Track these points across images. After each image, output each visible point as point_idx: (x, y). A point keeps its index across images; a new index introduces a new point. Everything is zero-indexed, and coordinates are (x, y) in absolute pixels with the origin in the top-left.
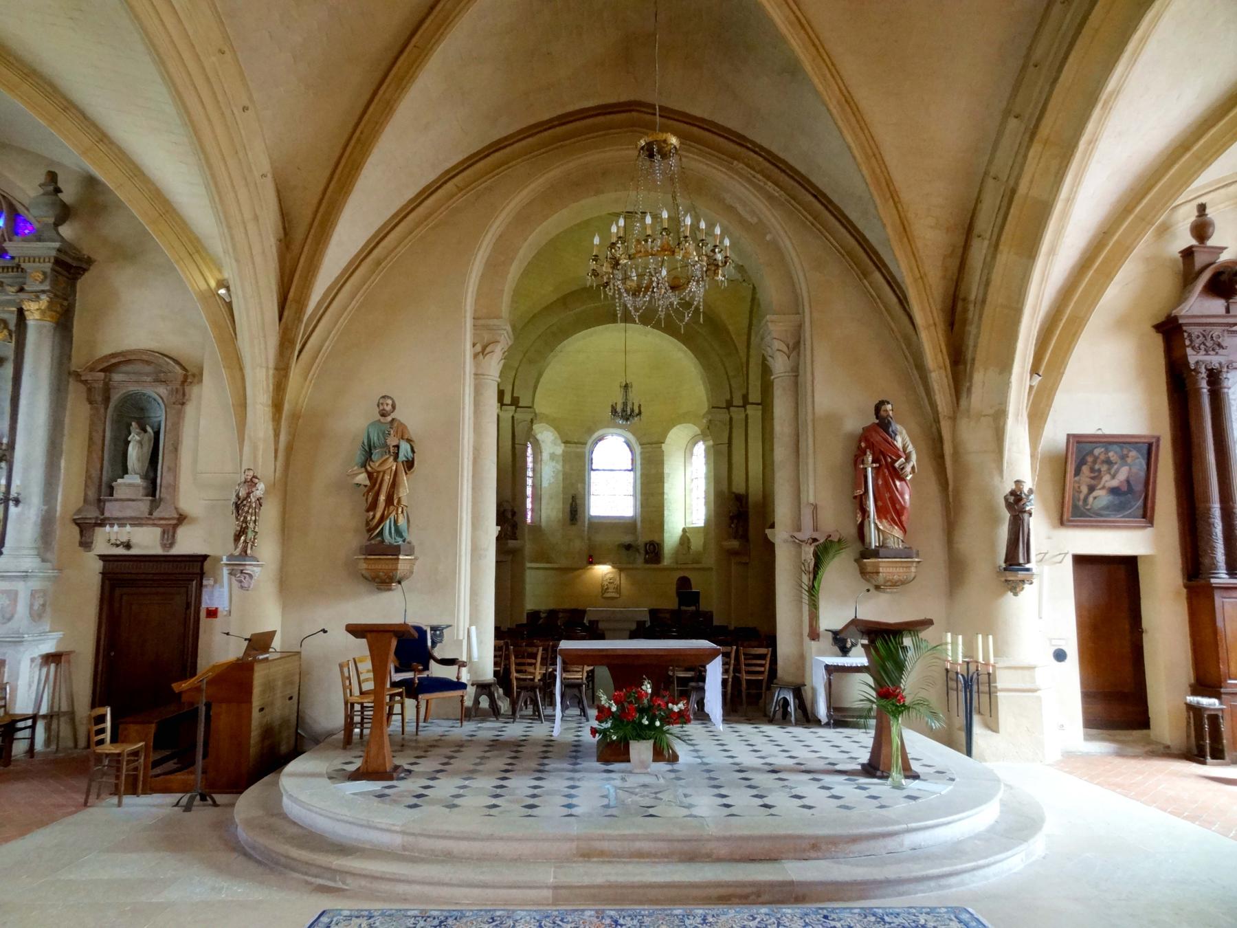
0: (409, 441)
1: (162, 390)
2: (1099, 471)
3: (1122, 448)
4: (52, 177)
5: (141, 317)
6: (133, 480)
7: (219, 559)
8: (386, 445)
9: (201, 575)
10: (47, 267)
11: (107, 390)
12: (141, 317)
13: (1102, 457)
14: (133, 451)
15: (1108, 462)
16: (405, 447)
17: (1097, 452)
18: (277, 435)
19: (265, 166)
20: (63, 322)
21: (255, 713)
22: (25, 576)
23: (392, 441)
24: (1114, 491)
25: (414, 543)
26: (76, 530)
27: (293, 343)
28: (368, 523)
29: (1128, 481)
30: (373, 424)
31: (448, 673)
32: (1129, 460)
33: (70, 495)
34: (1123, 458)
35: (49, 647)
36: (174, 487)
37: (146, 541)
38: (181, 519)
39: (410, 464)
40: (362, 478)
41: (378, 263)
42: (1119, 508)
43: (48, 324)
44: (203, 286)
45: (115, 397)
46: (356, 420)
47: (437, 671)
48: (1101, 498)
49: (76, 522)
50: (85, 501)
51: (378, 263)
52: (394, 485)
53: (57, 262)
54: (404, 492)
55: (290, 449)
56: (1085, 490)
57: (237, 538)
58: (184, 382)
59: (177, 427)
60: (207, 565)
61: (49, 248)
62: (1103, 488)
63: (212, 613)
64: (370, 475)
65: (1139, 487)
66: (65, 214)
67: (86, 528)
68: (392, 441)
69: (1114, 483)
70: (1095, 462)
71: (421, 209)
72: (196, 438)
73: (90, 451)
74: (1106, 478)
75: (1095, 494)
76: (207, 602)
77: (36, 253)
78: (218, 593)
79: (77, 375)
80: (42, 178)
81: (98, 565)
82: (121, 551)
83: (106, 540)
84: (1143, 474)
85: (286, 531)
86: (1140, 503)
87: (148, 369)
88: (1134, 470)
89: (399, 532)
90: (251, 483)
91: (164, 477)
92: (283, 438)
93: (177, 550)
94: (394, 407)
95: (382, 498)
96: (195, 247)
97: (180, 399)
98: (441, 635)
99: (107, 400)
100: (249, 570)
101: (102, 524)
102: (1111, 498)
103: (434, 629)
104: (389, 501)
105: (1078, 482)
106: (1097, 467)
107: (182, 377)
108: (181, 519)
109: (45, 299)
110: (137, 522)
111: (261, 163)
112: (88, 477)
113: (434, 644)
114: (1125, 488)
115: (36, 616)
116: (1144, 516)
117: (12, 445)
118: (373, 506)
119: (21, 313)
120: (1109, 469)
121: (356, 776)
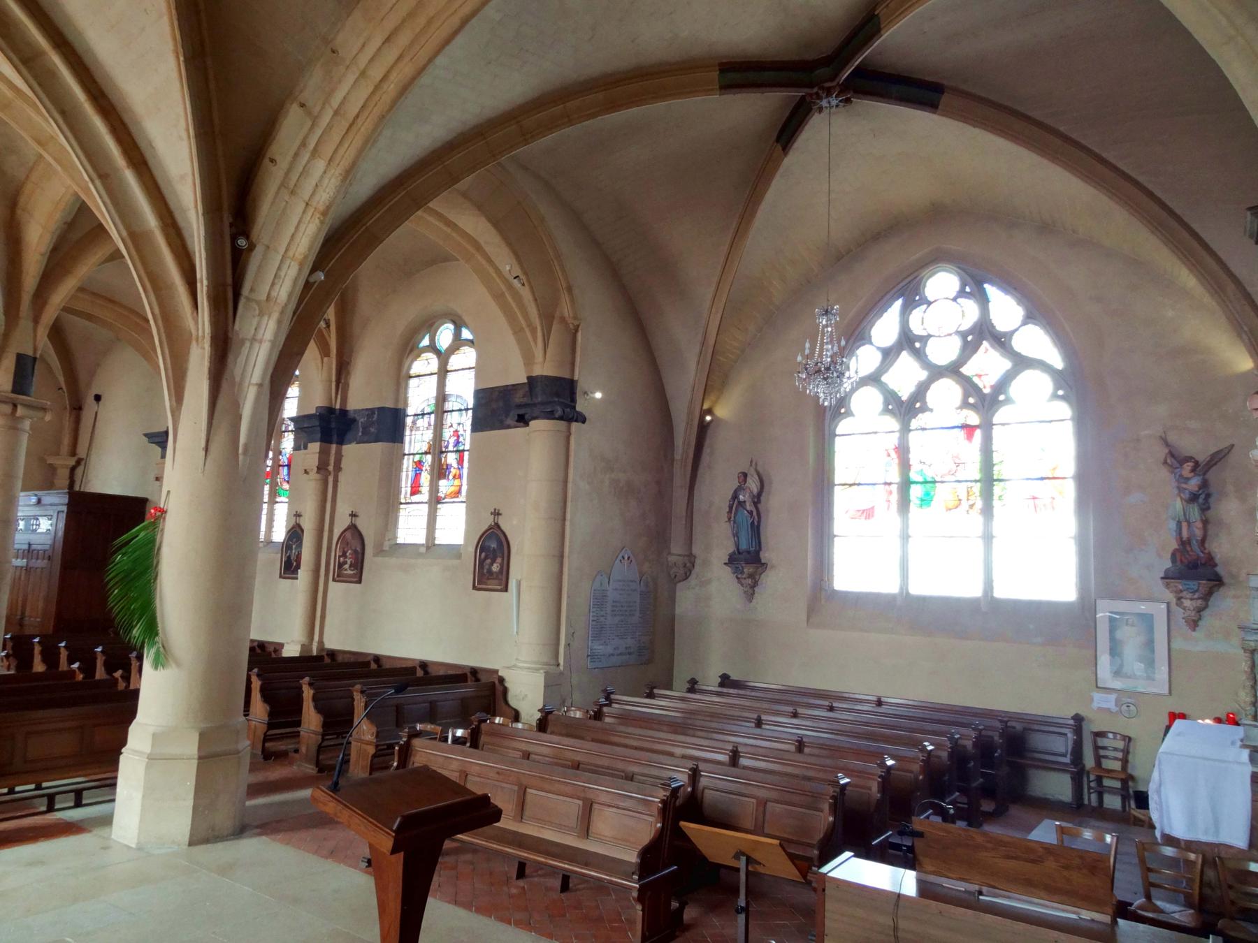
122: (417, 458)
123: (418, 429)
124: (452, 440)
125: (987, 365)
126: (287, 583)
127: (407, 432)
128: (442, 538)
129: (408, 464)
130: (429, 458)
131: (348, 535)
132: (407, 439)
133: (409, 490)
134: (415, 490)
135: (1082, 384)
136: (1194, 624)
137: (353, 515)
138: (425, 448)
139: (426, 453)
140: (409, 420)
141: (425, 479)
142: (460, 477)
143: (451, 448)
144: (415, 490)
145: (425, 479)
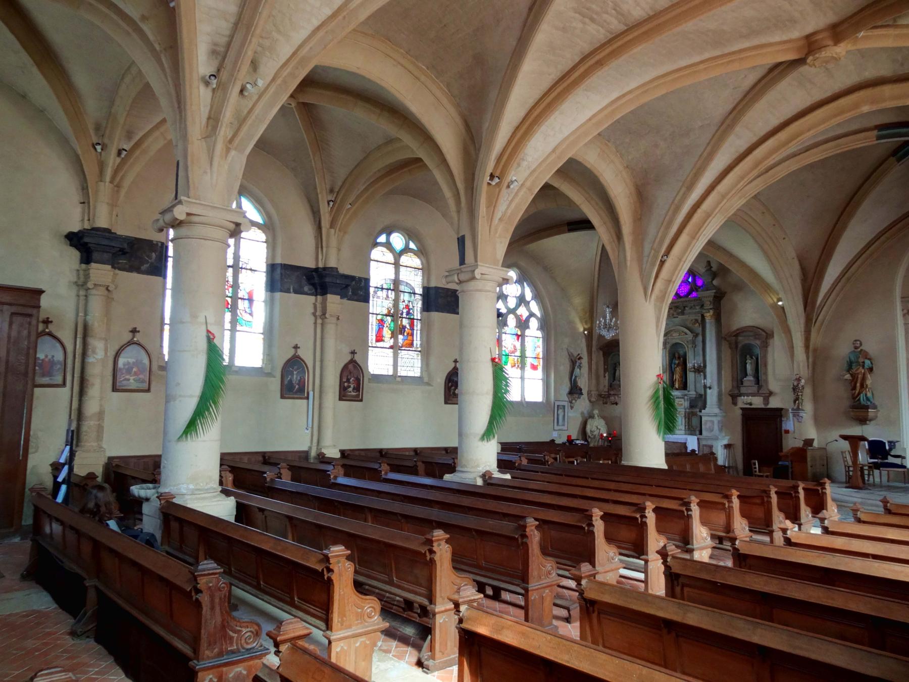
0: (870, 359)
1: (758, 342)
4: (709, 263)
5: (748, 313)
6: (750, 378)
7: (787, 410)
8: (858, 362)
9: (781, 416)
10: (711, 299)
11: (736, 343)
12: (748, 313)
14: (749, 367)
16: (867, 362)
18: (808, 358)
19: (794, 254)
20: (718, 318)
21: (809, 468)
22: (716, 415)
23: (861, 360)
25: (877, 403)
26: (730, 398)
27: (811, 320)
28: (853, 395)
30: (851, 352)
31: (898, 461)
33: (727, 385)
35: (725, 442)
36: (766, 381)
37: (757, 402)
38: (771, 393)
39: (871, 370)
40: (848, 376)
41: (849, 279)
43: (713, 320)
44: (771, 301)
45: (740, 346)
46: (843, 350)
47: (891, 460)
49: (731, 395)
50: (733, 387)
51: (849, 279)
52: (864, 379)
53: (715, 297)
54: (869, 382)
55: (814, 363)
57: (795, 402)
58: (767, 338)
59: (765, 357)
60: (783, 412)
61: (712, 293)
63: (787, 432)
64: (851, 375)
66: (714, 275)
67: (734, 397)
68: (861, 360)
71: (868, 252)
72: (774, 360)
73: (732, 366)
76: (784, 427)
77: (707, 295)
78: (789, 424)
79: (725, 339)
80: (705, 264)
81: (740, 412)
82: (748, 406)
83: (743, 401)
85: (816, 398)
87: (751, 334)
89: (868, 399)
90: (799, 380)
91: (762, 377)
92: (810, 360)
93: (769, 406)
94: (861, 344)
95: (858, 385)
96: (766, 287)
97: (765, 346)
98: (895, 445)
99: (737, 347)
100: (801, 415)
101: (740, 395)
103: (890, 442)
104: (862, 386)
107: (765, 336)
108: (771, 393)
109: (711, 312)
110: (753, 395)
111: (791, 254)
112: (733, 378)
113: (891, 449)
115: (721, 430)
117: (705, 366)
118: (854, 388)
119: (703, 317)
121: (846, 487)
122: (379, 317)
123: (378, 297)
124: (405, 311)
125: (523, 312)
126: (288, 402)
127: (371, 298)
128: (402, 372)
129: (373, 321)
130: (389, 319)
131: (351, 366)
132: (371, 302)
133: (374, 338)
134: (379, 338)
135: (544, 326)
136: (572, 408)
137: (353, 353)
138: (385, 312)
139: (386, 315)
140: (372, 290)
141: (387, 333)
142: (412, 335)
143: (404, 315)
144: (379, 338)
145: (387, 333)
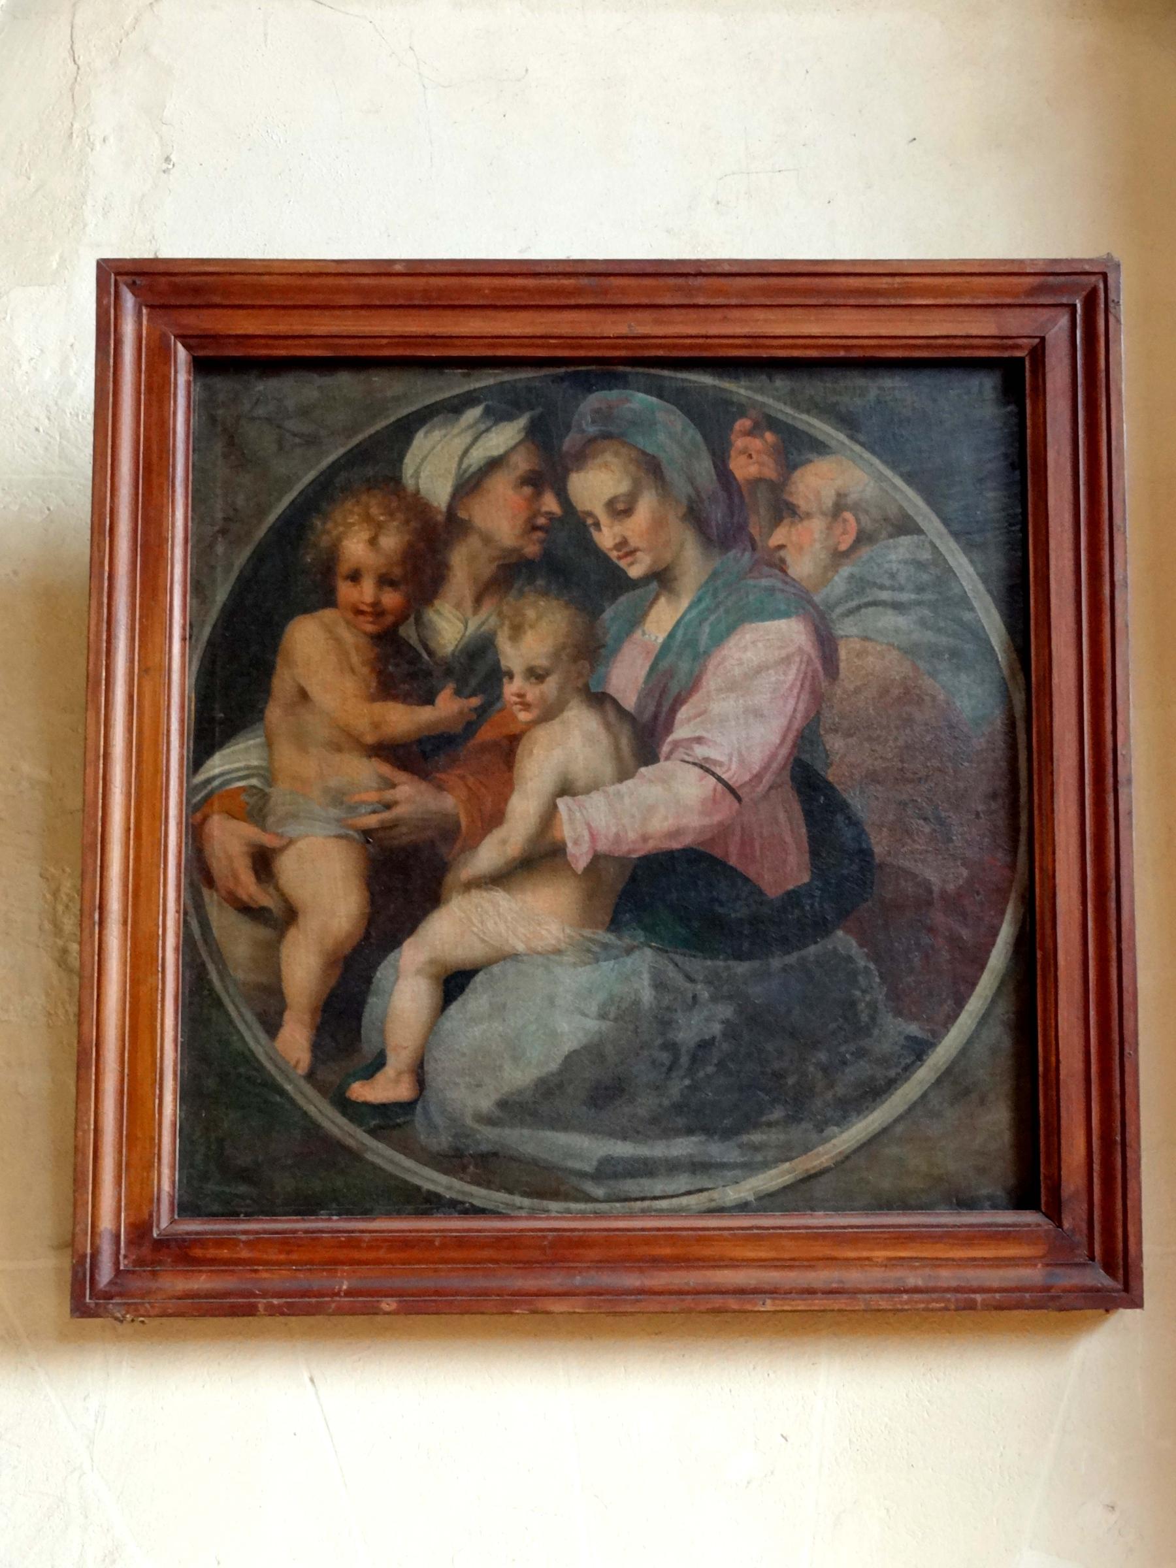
2: (479, 667)
3: (713, 424)
13: (501, 516)
15: (570, 568)
17: (433, 465)
24: (662, 896)
29: (806, 777)
32: (805, 549)
34: (731, 521)
42: (744, 1086)
48: (521, 980)
56: (327, 888)
62: (541, 858)
65: (936, 853)
69: (665, 805)
70: (421, 571)
74: (568, 744)
75: (452, 929)
84: (971, 699)
86: (972, 1022)
88: (879, 644)
102: (636, 972)
105: (255, 808)
106: (449, 626)
114: (783, 864)
116: (1031, 1184)
120: (589, 652)
